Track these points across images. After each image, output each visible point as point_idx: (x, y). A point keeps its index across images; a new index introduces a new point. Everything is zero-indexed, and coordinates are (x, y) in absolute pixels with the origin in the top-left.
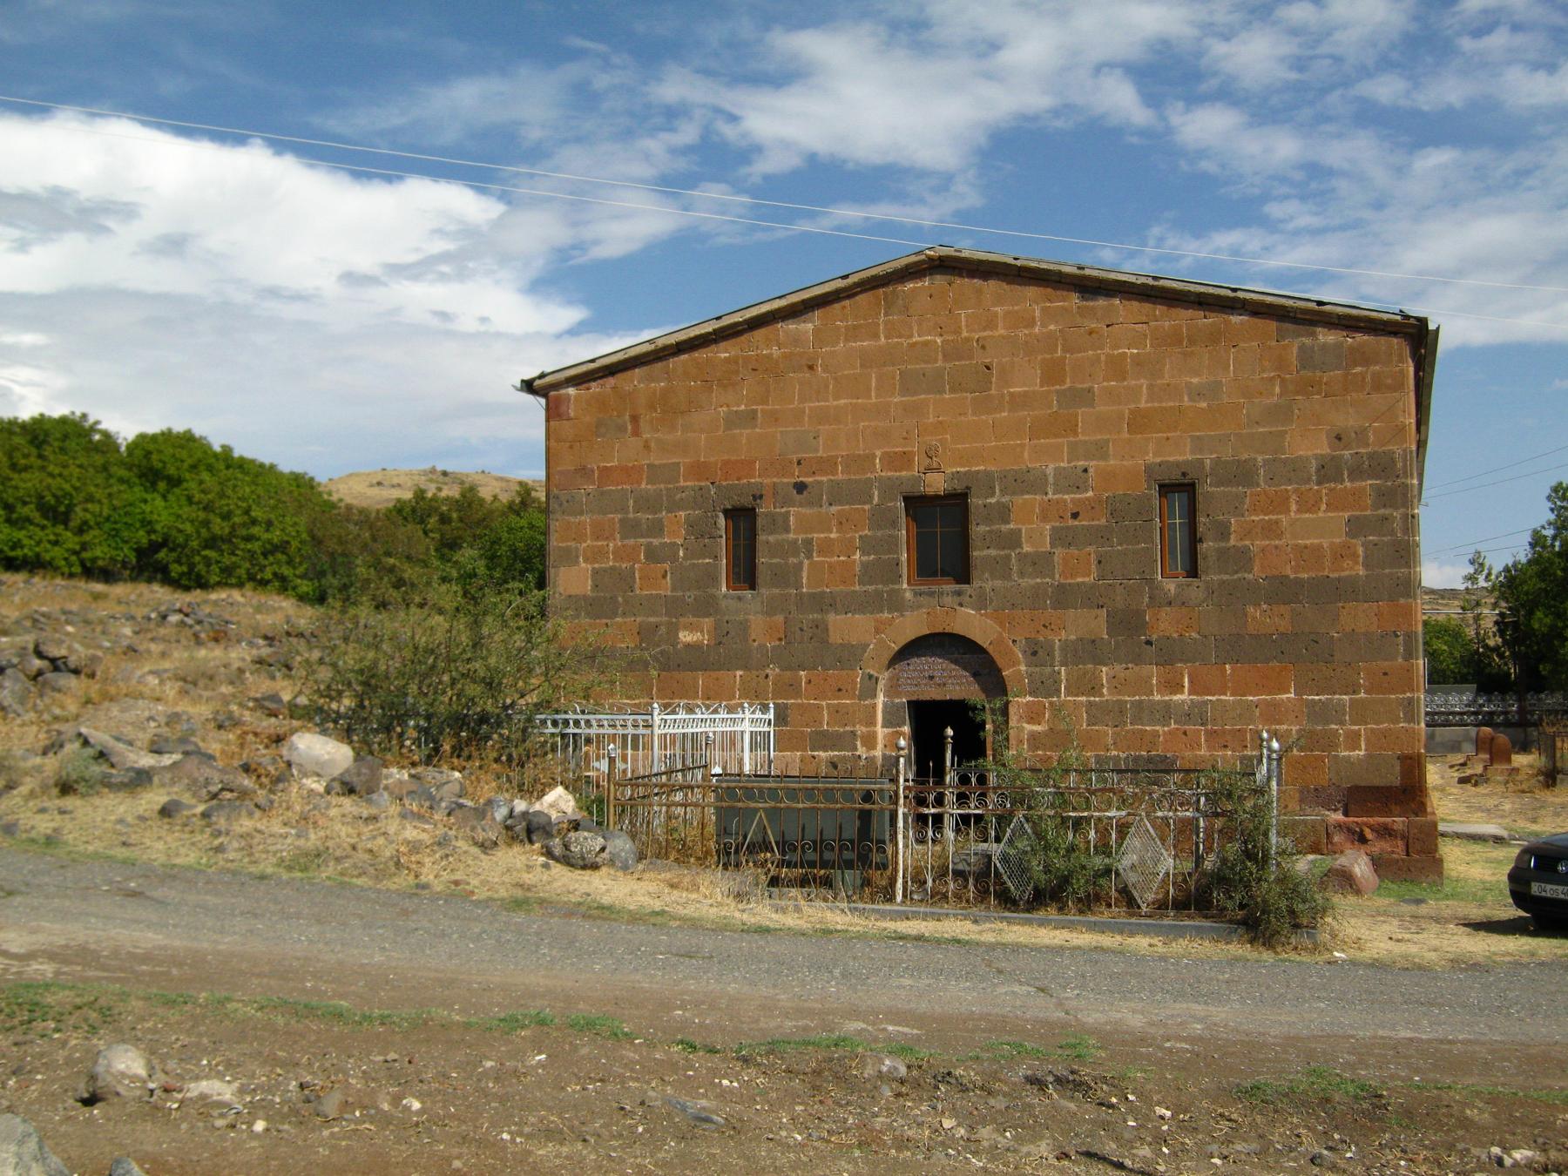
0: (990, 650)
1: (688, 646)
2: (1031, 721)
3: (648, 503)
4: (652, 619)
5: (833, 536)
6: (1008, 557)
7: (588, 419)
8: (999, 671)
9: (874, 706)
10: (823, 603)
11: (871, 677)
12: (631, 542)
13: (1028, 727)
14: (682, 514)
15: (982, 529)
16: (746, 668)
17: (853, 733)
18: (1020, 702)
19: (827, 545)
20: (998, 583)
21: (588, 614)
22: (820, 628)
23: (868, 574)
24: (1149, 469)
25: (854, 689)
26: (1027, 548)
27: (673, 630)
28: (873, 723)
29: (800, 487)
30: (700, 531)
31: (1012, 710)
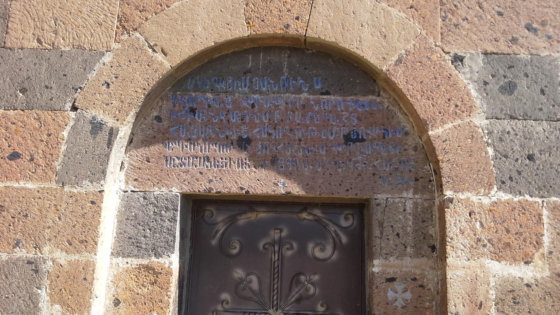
0: (399, 79)
2: (502, 251)
8: (422, 126)
9: (96, 202)
11: (96, 127)
13: (500, 270)
17: (34, 266)
18: (469, 206)
25: (49, 157)
28: (86, 241)
31: (455, 222)
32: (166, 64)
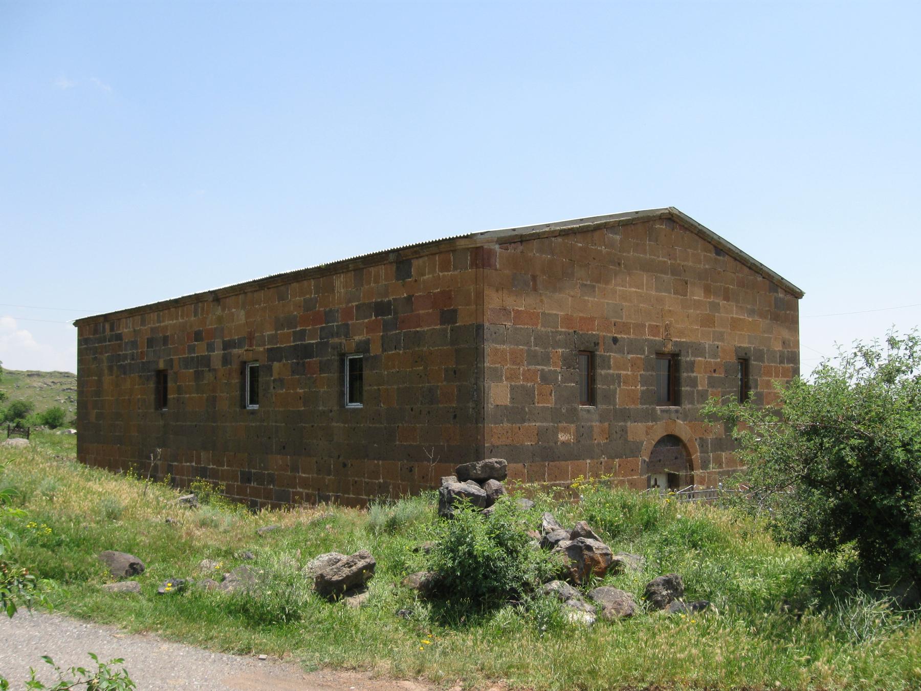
1: (563, 443)
3: (541, 340)
4: (544, 424)
5: (629, 373)
6: (693, 392)
7: (507, 272)
10: (625, 415)
12: (533, 367)
14: (560, 350)
15: (685, 375)
16: (592, 458)
19: (626, 377)
20: (690, 406)
21: (508, 421)
22: (624, 430)
23: (646, 398)
24: (738, 349)
26: (700, 388)
27: (556, 431)
29: (615, 340)
30: (568, 362)
32: (654, 443)
